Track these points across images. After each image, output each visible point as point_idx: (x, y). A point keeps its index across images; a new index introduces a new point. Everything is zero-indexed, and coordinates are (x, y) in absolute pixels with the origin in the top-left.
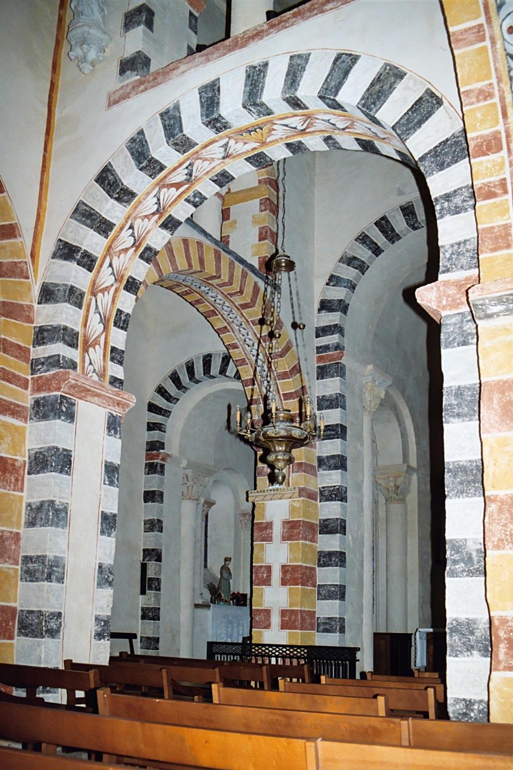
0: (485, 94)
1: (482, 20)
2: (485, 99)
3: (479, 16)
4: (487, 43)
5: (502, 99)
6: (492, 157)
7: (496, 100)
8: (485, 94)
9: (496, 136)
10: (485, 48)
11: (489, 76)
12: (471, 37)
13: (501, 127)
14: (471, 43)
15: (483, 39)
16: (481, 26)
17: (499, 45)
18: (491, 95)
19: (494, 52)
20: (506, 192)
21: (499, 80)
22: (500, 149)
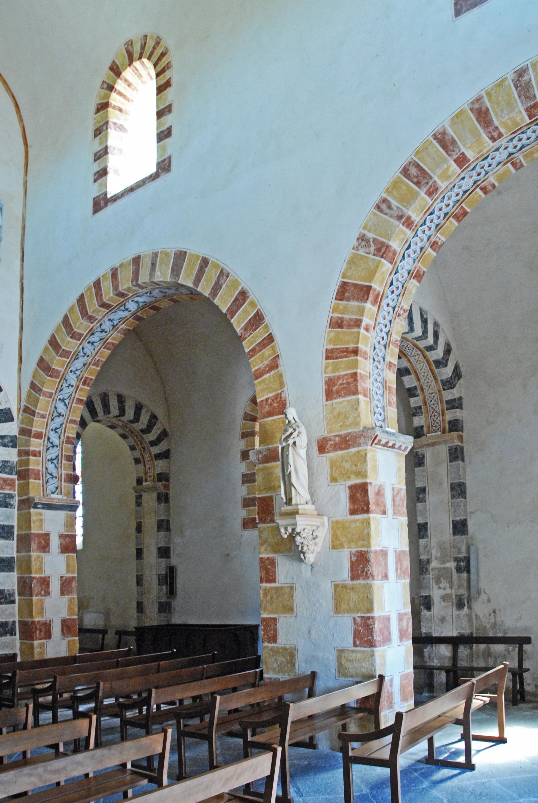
0: (43, 417)
1: (54, 392)
2: (43, 418)
3: (54, 390)
4: (51, 400)
5: (47, 421)
6: (38, 440)
7: (46, 420)
8: (43, 417)
9: (41, 433)
10: (50, 401)
11: (47, 411)
12: (48, 395)
13: (44, 431)
14: (47, 397)
15: (51, 397)
16: (52, 393)
17: (54, 402)
18: (45, 418)
19: (52, 403)
20: (40, 456)
21: (49, 414)
22: (41, 438)
